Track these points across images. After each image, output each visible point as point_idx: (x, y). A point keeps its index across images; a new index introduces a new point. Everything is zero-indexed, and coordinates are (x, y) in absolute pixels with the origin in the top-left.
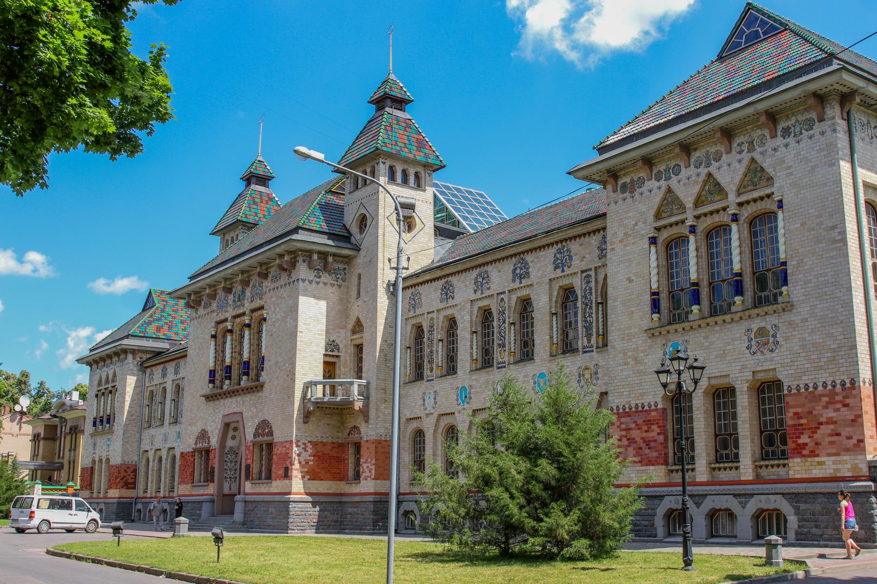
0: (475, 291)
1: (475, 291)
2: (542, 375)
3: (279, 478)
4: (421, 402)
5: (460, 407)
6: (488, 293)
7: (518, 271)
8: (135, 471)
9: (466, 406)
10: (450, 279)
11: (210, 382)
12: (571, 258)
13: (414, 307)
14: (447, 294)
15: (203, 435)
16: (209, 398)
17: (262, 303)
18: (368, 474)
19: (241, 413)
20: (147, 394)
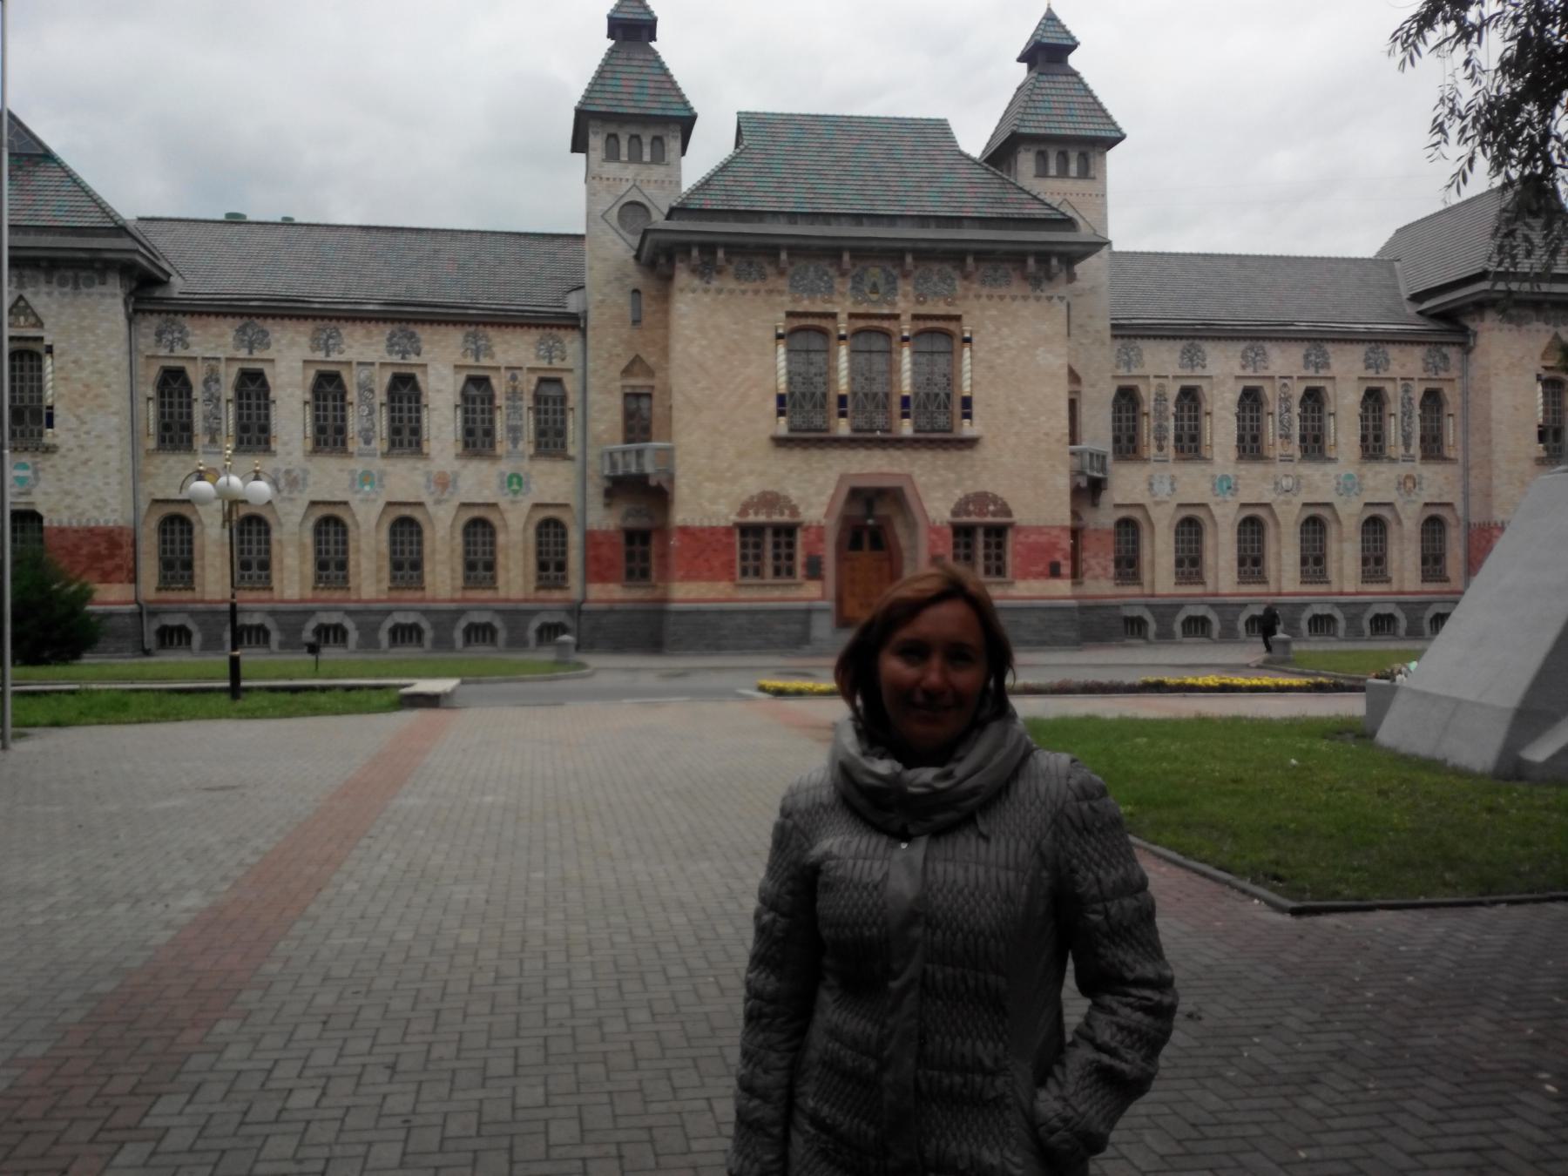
0: (1244, 367)
1: (1244, 367)
2: (1349, 476)
3: (1038, 576)
4: (1145, 486)
5: (1219, 499)
6: (1266, 373)
7: (1313, 358)
8: (134, 544)
9: (1229, 498)
10: (1197, 342)
11: (781, 413)
12: (1388, 361)
13: (1128, 364)
14: (1191, 360)
15: (769, 500)
16: (779, 442)
17: (953, 311)
18: (1098, 571)
19: (909, 477)
20: (154, 372)
